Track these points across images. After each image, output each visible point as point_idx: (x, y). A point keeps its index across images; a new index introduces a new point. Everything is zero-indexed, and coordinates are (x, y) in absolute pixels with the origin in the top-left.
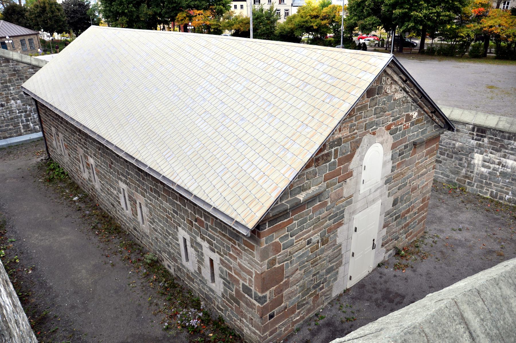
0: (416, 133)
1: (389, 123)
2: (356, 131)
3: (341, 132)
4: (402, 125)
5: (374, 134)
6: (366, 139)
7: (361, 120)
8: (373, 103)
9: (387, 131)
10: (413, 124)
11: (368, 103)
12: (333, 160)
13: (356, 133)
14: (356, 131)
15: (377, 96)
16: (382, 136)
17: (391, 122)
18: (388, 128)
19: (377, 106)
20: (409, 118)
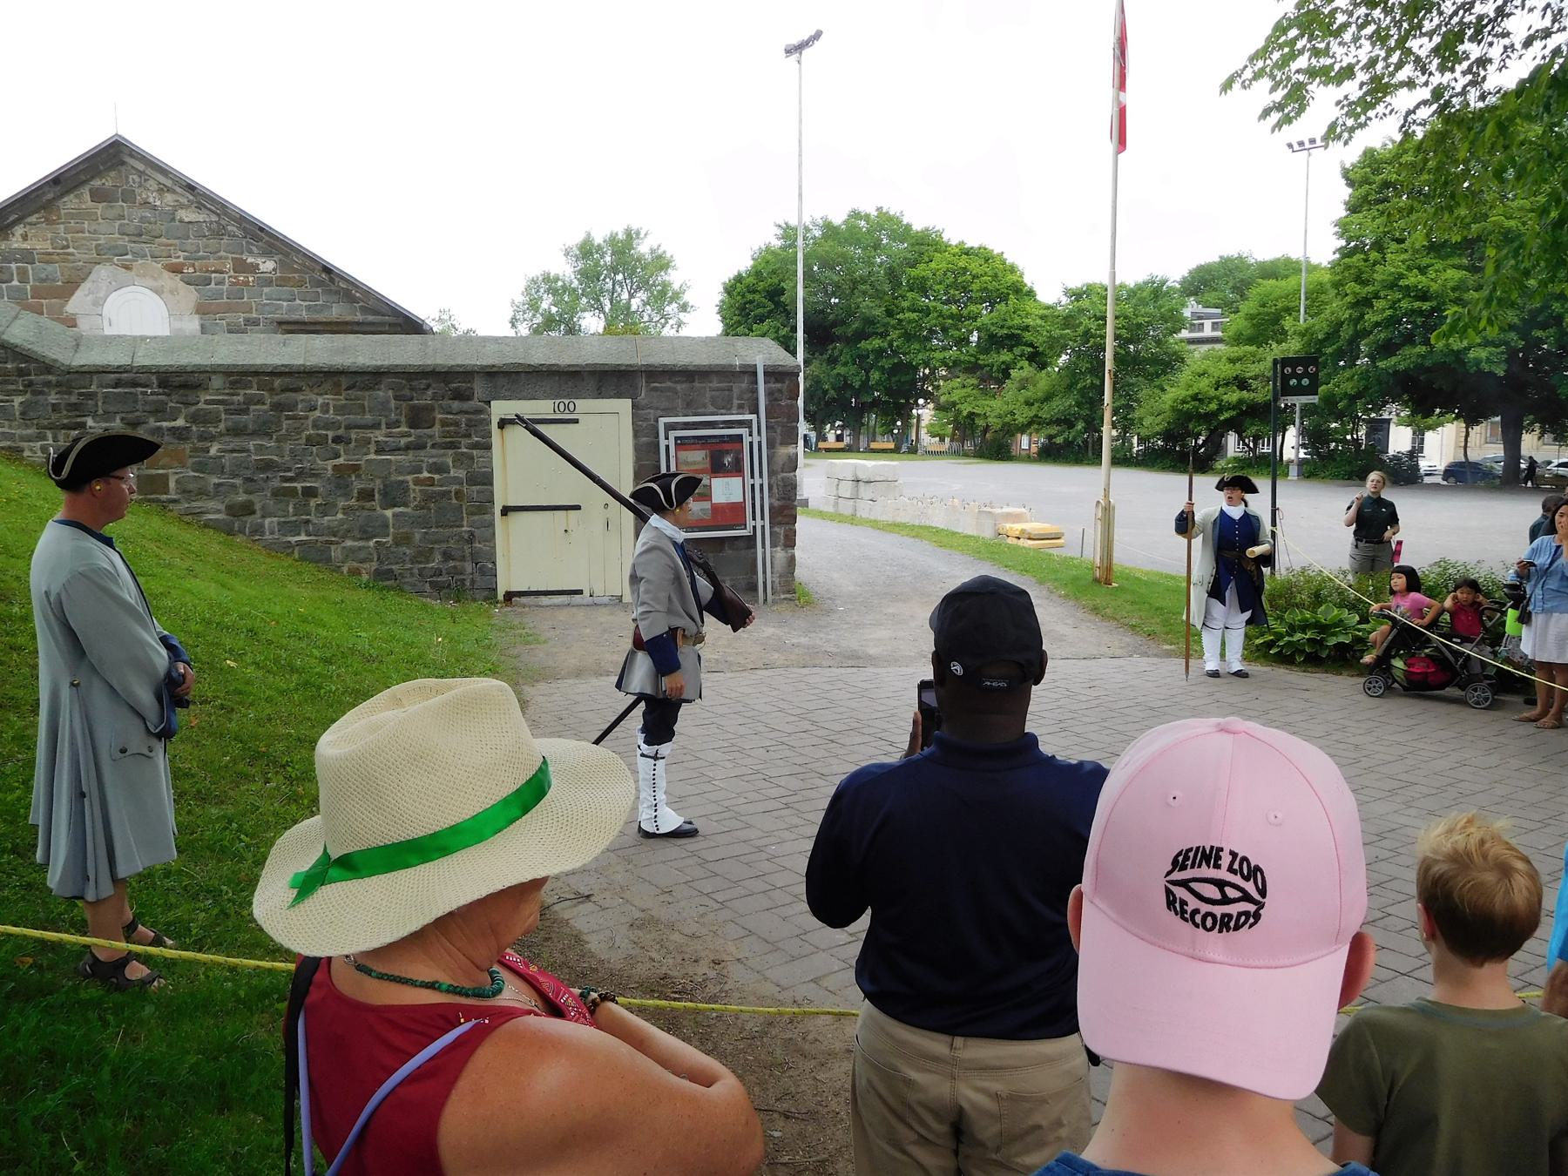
0: (285, 304)
1: (174, 260)
2: (71, 250)
3: (29, 242)
4: (226, 276)
5: (127, 268)
6: (102, 273)
7: (80, 235)
8: (112, 213)
9: (172, 275)
10: (269, 282)
11: (99, 212)
12: (15, 283)
13: (73, 254)
14: (71, 250)
15: (121, 203)
16: (155, 279)
17: (181, 260)
18: (176, 270)
19: (126, 221)
20: (241, 267)
